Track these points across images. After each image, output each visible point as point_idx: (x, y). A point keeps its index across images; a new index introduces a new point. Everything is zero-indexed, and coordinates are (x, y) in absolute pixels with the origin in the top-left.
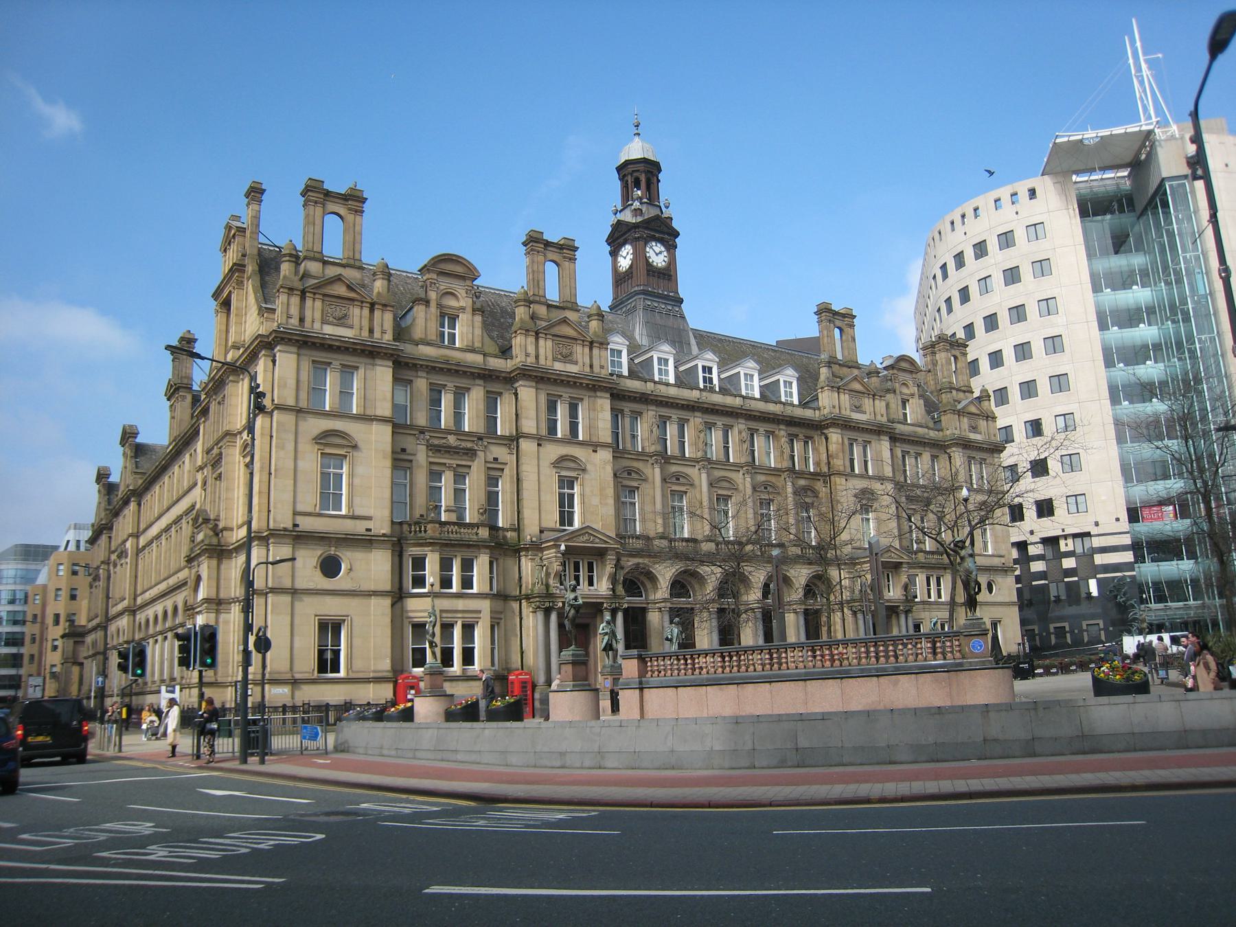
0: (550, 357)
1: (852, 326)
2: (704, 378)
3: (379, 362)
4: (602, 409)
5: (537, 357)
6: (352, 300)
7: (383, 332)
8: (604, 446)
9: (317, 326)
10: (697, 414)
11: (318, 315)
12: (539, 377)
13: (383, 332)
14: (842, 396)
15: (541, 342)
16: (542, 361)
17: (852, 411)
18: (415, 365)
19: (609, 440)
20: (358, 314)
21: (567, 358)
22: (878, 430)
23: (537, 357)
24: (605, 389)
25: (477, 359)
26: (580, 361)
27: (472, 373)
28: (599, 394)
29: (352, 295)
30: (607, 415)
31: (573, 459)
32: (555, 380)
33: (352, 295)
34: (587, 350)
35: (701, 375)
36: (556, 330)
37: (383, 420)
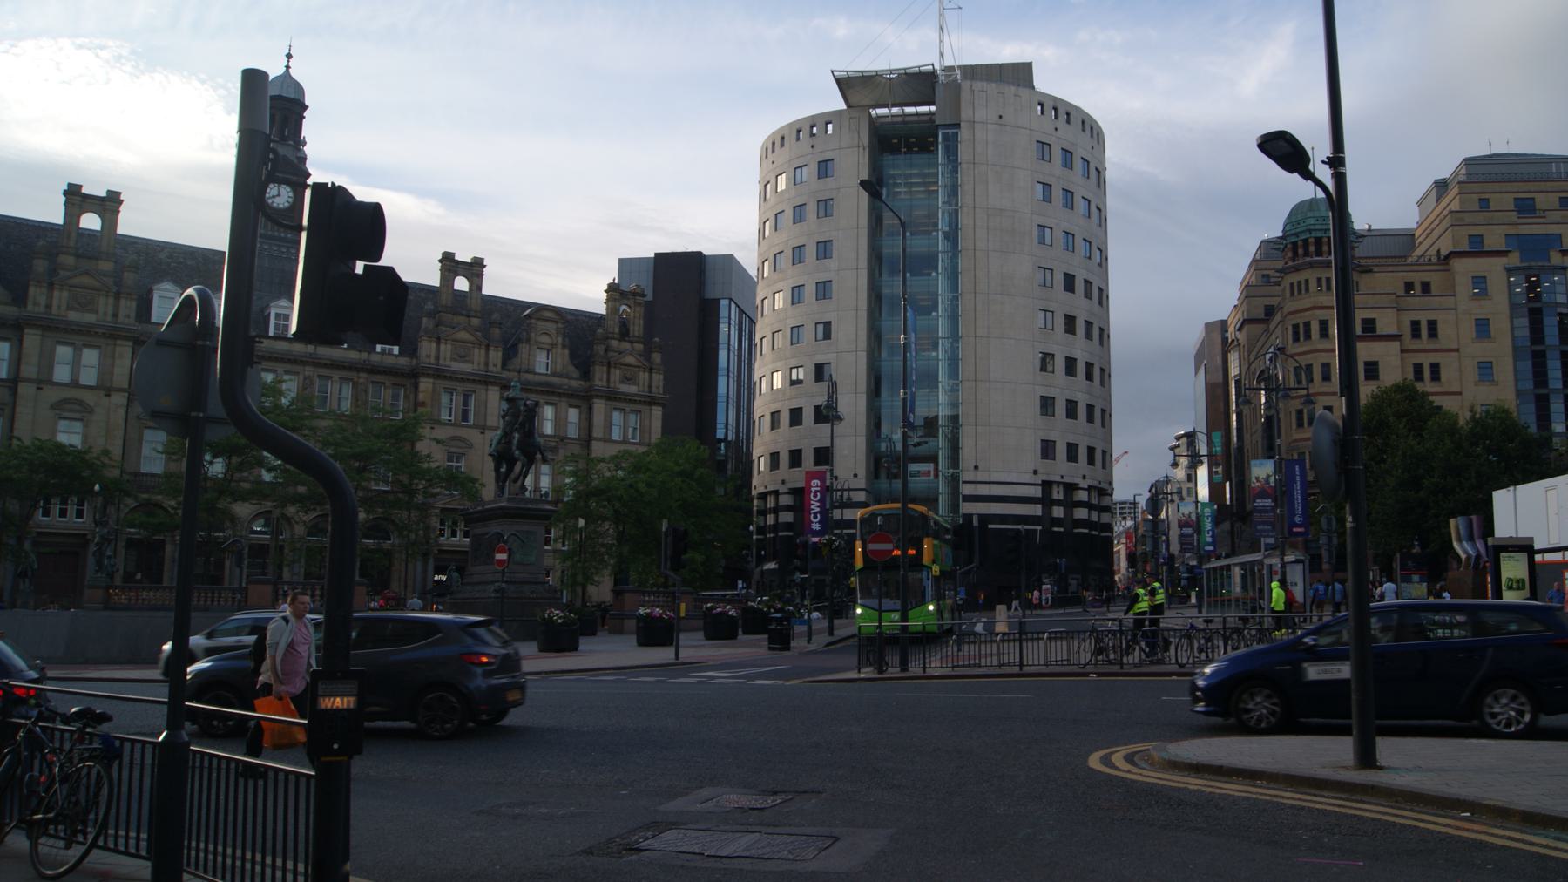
1: (481, 275)
2: (277, 326)
8: (121, 390)
14: (442, 347)
15: (56, 293)
16: (54, 310)
17: (453, 359)
19: (126, 386)
24: (126, 338)
31: (80, 402)
34: (111, 301)
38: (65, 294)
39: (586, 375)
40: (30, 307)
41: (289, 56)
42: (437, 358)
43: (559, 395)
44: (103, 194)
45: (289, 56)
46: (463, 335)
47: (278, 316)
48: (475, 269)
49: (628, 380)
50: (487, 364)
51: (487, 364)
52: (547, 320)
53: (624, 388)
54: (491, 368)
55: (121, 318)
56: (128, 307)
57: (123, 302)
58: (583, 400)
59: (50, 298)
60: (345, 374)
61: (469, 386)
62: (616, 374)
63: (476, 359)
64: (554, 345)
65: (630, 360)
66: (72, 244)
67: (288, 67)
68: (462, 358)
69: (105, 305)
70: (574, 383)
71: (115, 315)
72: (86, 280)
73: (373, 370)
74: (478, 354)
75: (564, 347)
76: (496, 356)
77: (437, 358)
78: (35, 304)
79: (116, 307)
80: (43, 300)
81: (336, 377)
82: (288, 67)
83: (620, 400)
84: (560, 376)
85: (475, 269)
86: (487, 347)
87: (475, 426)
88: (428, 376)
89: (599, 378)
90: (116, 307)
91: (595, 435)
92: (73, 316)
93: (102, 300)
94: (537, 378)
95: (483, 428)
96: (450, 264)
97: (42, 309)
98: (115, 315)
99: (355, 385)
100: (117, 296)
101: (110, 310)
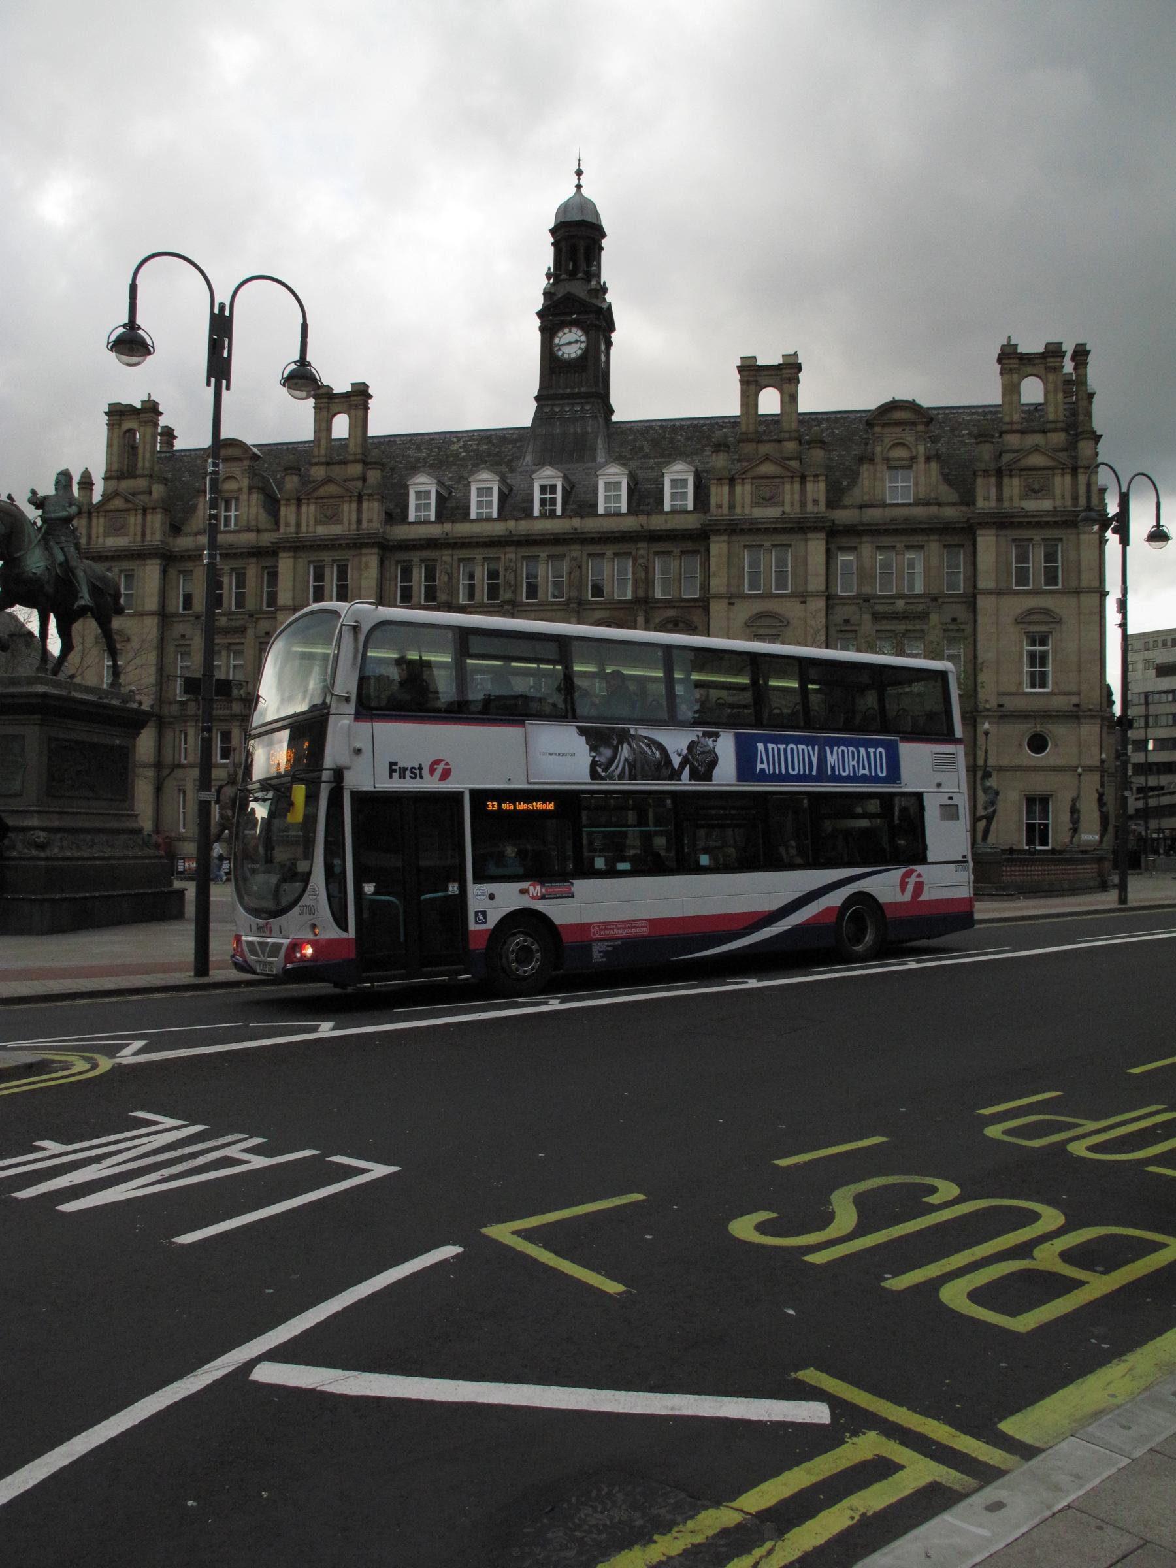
0: (312, 522)
2: (543, 502)
3: (149, 562)
4: (367, 567)
5: (298, 525)
6: (128, 510)
7: (153, 534)
9: (101, 540)
10: (508, 549)
11: (101, 531)
12: (298, 547)
13: (153, 534)
14: (738, 489)
15: (304, 509)
17: (754, 504)
18: (189, 557)
20: (134, 521)
21: (333, 518)
22: (801, 527)
23: (298, 525)
25: (249, 538)
26: (346, 521)
27: (242, 553)
28: (364, 551)
29: (130, 506)
30: (373, 572)
32: (311, 546)
33: (130, 506)
34: (354, 506)
35: (537, 496)
36: (315, 495)
37: (152, 614)
38: (312, 508)
39: (968, 499)
40: (282, 530)
41: (579, 173)
42: (732, 506)
43: (923, 531)
44: (349, 389)
45: (579, 173)
46: (767, 469)
47: (543, 489)
48: (787, 374)
49: (1032, 492)
50: (803, 504)
51: (803, 504)
52: (898, 424)
53: (1031, 505)
54: (810, 507)
55: (365, 524)
56: (373, 511)
57: (365, 505)
58: (959, 535)
59: (299, 514)
60: (618, 548)
61: (783, 539)
62: (1014, 486)
63: (787, 498)
64: (913, 459)
65: (1037, 460)
66: (323, 452)
67: (579, 186)
68: (769, 501)
69: (348, 510)
70: (950, 513)
71: (359, 522)
72: (331, 489)
73: (654, 537)
74: (790, 492)
75: (928, 459)
76: (817, 490)
77: (732, 506)
78: (287, 525)
79: (359, 511)
80: (292, 519)
81: (609, 553)
82: (579, 186)
83: (1020, 525)
84: (926, 503)
85: (787, 374)
86: (803, 479)
87: (793, 595)
88: (718, 532)
89: (985, 499)
90: (359, 511)
91: (982, 584)
92: (321, 530)
93: (346, 507)
94: (889, 513)
95: (803, 597)
96: (753, 375)
97: (292, 529)
98: (359, 522)
99: (635, 559)
100: (360, 502)
101: (354, 517)
